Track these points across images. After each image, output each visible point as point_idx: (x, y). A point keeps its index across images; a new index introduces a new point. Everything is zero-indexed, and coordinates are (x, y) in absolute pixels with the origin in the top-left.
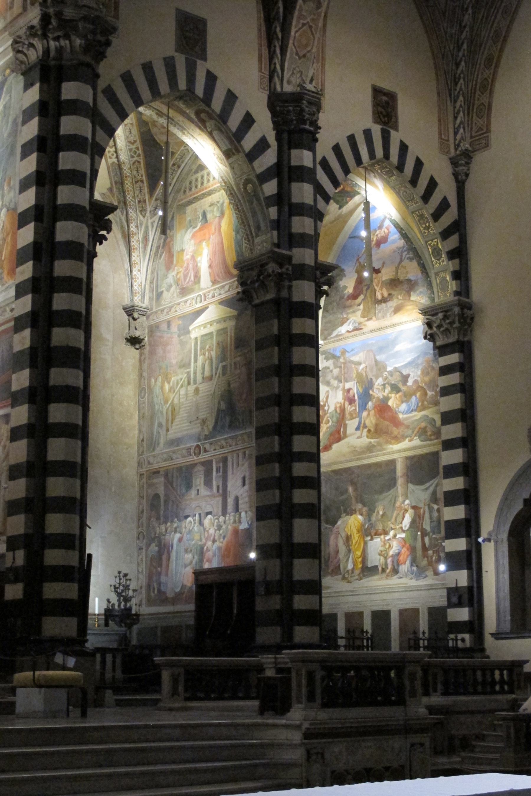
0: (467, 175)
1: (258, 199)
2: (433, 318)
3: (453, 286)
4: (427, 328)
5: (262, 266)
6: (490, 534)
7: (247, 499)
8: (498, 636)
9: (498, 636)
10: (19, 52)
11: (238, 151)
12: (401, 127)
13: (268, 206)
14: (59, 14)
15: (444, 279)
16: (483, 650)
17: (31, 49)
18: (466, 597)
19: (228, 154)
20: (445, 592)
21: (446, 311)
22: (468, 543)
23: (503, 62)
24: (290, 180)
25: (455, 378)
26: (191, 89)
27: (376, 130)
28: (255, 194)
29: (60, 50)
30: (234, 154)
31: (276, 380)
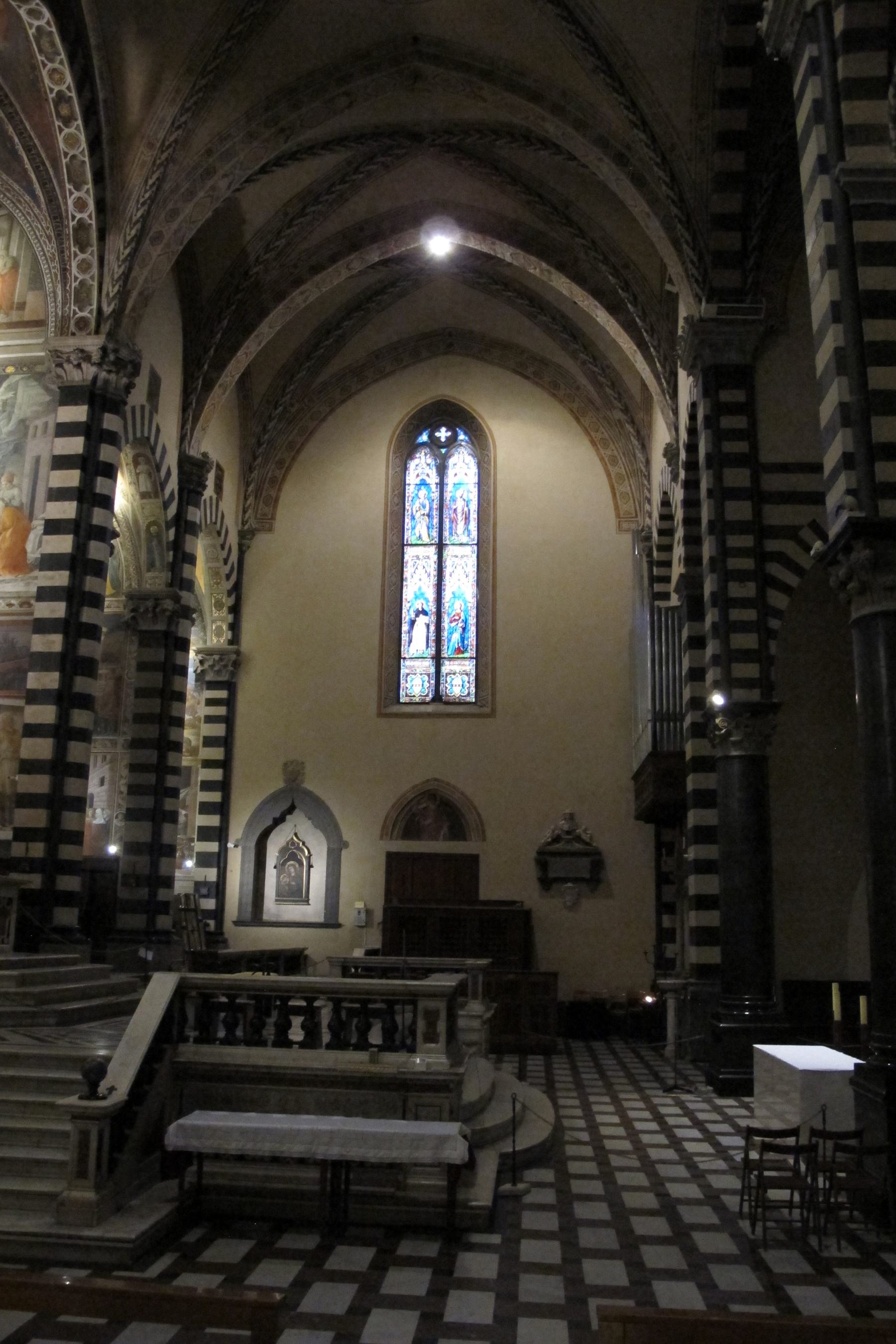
0: (249, 547)
1: (160, 542)
2: (208, 657)
3: (229, 635)
4: (199, 664)
5: (157, 599)
6: (237, 840)
7: (105, 798)
8: (238, 923)
9: (238, 923)
10: (59, 365)
11: (156, 496)
12: (223, 499)
13: (168, 550)
14: (116, 351)
15: (221, 627)
16: (222, 934)
17: (79, 371)
18: (214, 890)
19: (144, 496)
20: (192, 885)
21: (222, 655)
22: (220, 846)
23: (293, 470)
24: (185, 532)
25: (221, 711)
26: (148, 439)
27: (215, 496)
28: (158, 535)
29: (106, 382)
30: (150, 497)
31: (158, 701)
